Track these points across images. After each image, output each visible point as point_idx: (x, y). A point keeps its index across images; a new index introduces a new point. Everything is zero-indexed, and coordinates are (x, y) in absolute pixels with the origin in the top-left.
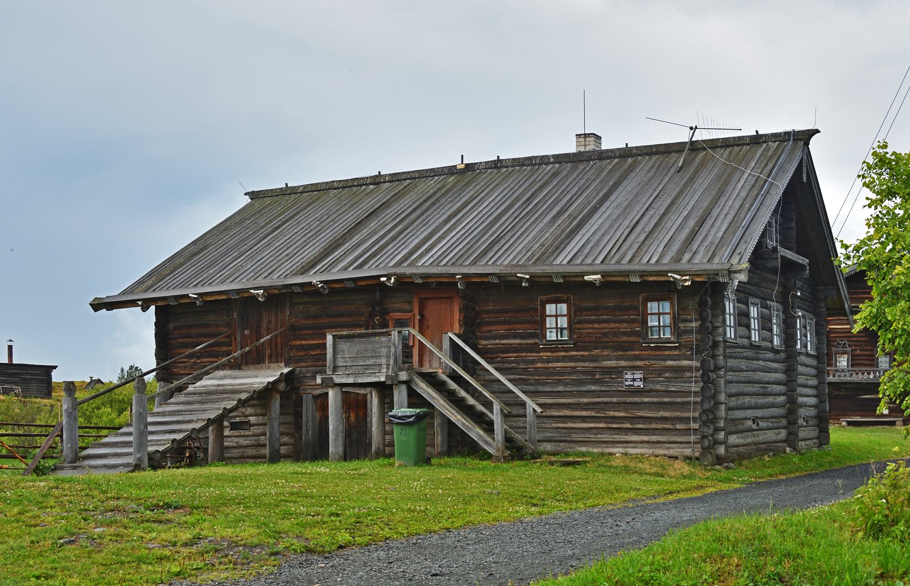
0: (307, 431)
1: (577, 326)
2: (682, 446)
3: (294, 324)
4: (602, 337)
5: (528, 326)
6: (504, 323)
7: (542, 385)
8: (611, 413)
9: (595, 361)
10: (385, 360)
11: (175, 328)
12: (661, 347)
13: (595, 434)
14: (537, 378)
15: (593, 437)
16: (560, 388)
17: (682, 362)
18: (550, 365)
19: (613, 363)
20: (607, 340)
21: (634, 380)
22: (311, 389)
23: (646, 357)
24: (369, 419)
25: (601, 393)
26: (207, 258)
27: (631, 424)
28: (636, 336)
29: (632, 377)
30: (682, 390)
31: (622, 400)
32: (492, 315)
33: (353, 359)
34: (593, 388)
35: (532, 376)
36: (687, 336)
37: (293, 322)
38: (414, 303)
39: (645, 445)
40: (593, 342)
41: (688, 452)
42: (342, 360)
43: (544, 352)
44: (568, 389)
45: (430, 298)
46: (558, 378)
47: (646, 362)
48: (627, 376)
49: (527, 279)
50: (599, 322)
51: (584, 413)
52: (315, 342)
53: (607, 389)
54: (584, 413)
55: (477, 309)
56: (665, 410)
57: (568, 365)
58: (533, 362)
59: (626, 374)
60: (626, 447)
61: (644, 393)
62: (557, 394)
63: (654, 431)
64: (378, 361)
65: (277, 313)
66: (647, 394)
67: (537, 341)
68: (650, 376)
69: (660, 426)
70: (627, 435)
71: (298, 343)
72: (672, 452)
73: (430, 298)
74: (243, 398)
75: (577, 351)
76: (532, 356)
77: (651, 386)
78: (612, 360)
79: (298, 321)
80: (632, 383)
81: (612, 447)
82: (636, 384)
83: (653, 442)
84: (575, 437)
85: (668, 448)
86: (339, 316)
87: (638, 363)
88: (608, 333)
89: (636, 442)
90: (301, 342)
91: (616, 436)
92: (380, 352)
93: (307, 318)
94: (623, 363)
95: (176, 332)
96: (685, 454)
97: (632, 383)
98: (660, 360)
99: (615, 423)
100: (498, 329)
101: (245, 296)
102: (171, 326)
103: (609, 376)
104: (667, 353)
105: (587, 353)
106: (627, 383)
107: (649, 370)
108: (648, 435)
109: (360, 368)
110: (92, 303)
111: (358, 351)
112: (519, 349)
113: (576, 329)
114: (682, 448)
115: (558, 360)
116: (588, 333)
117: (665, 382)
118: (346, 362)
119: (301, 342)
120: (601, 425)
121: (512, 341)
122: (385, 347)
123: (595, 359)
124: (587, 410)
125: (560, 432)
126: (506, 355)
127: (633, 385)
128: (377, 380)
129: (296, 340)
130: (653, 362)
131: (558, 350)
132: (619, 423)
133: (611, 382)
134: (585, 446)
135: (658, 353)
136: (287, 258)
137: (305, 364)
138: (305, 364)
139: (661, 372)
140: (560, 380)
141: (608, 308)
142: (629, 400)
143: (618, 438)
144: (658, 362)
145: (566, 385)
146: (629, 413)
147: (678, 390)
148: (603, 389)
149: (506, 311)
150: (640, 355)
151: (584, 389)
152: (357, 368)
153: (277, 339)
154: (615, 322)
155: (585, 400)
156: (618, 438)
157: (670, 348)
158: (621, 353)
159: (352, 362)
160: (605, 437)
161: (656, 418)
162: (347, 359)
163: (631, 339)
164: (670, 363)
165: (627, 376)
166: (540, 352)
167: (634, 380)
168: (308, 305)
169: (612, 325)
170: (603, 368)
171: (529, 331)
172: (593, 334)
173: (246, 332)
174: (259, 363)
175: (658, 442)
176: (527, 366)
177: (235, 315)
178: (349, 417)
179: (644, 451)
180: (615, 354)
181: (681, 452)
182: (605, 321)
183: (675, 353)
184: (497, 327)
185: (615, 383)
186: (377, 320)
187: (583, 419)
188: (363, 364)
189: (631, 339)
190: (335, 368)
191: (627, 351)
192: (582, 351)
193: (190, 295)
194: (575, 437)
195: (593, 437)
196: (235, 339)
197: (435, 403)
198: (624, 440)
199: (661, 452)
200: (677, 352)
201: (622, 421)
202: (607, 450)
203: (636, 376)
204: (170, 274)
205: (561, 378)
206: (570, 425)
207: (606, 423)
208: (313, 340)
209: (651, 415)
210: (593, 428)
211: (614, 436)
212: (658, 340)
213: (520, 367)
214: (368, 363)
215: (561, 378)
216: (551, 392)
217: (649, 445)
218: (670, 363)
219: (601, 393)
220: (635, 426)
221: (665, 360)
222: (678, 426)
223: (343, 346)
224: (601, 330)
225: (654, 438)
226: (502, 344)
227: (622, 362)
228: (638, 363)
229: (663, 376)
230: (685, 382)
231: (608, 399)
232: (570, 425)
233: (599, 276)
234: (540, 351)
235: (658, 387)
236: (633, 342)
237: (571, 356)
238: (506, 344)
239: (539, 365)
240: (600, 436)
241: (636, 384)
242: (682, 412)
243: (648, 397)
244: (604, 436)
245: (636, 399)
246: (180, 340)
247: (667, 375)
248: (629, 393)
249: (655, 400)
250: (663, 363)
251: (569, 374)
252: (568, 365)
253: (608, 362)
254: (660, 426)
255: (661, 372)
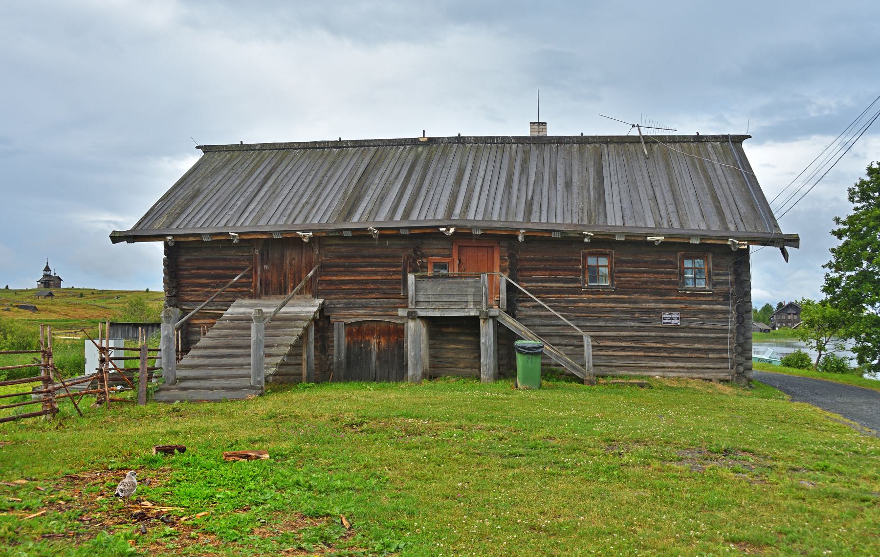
0: (339, 353)
1: (618, 275)
2: (714, 371)
3: (324, 262)
4: (642, 284)
5: (569, 273)
6: (546, 269)
7: (583, 321)
8: (650, 345)
9: (635, 303)
10: (472, 298)
11: (188, 261)
12: (696, 294)
13: (634, 361)
14: (578, 315)
15: (632, 363)
16: (601, 324)
17: (716, 306)
18: (591, 305)
19: (652, 305)
20: (646, 286)
21: (671, 319)
22: (343, 318)
23: (682, 301)
24: (405, 345)
25: (639, 329)
26: (324, 208)
27: (668, 353)
28: (674, 285)
29: (669, 316)
30: (715, 328)
31: (659, 334)
32: (533, 263)
33: (436, 296)
34: (632, 324)
35: (575, 313)
36: (721, 287)
37: (322, 260)
38: (454, 250)
39: (681, 370)
40: (632, 288)
41: (722, 375)
42: (423, 296)
43: (586, 294)
44: (608, 325)
45: (466, 246)
46: (599, 315)
47: (683, 306)
48: (664, 316)
49: (591, 236)
50: (637, 272)
51: (623, 344)
52: (347, 278)
53: (645, 325)
54: (623, 344)
55: (518, 257)
56: (699, 343)
57: (609, 305)
58: (574, 302)
59: (664, 314)
60: (664, 371)
61: (679, 330)
62: (597, 328)
63: (689, 359)
64: (464, 299)
65: (302, 253)
66: (682, 330)
67: (579, 285)
68: (686, 316)
69: (694, 355)
70: (664, 362)
71: (328, 278)
72: (706, 376)
73: (466, 246)
74: (305, 326)
75: (617, 294)
76: (571, 297)
77: (686, 324)
78: (651, 303)
79: (328, 260)
80: (670, 321)
81: (651, 371)
82: (673, 322)
83: (688, 368)
84: (615, 362)
85: (703, 373)
86: (375, 257)
87: (675, 306)
88: (647, 281)
89: (671, 368)
90: (331, 278)
91: (654, 363)
92: (467, 291)
93: (339, 257)
94: (661, 305)
95: (188, 264)
96: (718, 378)
97: (670, 321)
98: (696, 304)
99: (653, 352)
100: (540, 274)
101: (288, 236)
102: (183, 258)
103: (647, 315)
104: (701, 299)
105: (627, 297)
106: (665, 321)
107: (685, 312)
108: (684, 362)
109: (444, 303)
110: (113, 235)
111: (442, 289)
112: (560, 291)
113: (616, 277)
114: (716, 373)
115: (598, 301)
116: (628, 281)
117: (700, 321)
118: (428, 298)
119: (331, 278)
120: (639, 354)
121: (554, 285)
122: (471, 287)
123: (634, 302)
124: (627, 341)
125: (600, 359)
126: (548, 295)
127: (671, 323)
128: (467, 314)
129: (326, 275)
130: (690, 305)
131: (599, 293)
132: (657, 352)
133: (650, 320)
134: (625, 370)
135: (693, 298)
136: (309, 207)
137: (336, 297)
138: (336, 297)
139: (696, 313)
140: (600, 317)
141: (647, 262)
142: (666, 334)
143: (656, 364)
144: (693, 306)
145: (606, 321)
146: (667, 344)
147: (711, 327)
148: (642, 325)
149: (547, 260)
150: (676, 299)
151: (624, 324)
152: (441, 303)
153: (301, 273)
154: (654, 273)
155: (625, 334)
156: (656, 364)
157: (705, 295)
158: (660, 298)
159: (435, 298)
160: (644, 363)
161: (690, 349)
162: (430, 296)
163: (668, 287)
164: (704, 306)
165: (664, 316)
166: (582, 294)
167: (671, 319)
168: (339, 247)
169: (651, 275)
170: (642, 308)
171: (570, 277)
172: (633, 281)
173: (265, 266)
174: (281, 294)
175: (692, 368)
176: (568, 305)
177: (257, 252)
178: (380, 342)
179: (681, 374)
180: (653, 298)
181: (715, 376)
182: (644, 272)
183: (708, 299)
184: (538, 273)
185: (654, 320)
186: (419, 262)
187: (622, 348)
188: (448, 300)
189: (668, 287)
190: (417, 303)
191: (665, 296)
192: (622, 295)
193: (230, 233)
194: (615, 362)
195: (632, 363)
196: (256, 273)
197: (522, 335)
198: (661, 365)
199: (696, 375)
200: (710, 299)
201: (659, 351)
202: (646, 374)
203: (673, 316)
204: (182, 212)
205: (601, 315)
206: (610, 353)
207: (644, 352)
208: (346, 276)
209: (686, 347)
210: (631, 356)
211: (652, 363)
212: (694, 289)
213: (562, 305)
214: (452, 299)
215: (601, 315)
216: (591, 326)
217: (685, 370)
218: (704, 306)
219: (639, 329)
220: (672, 355)
221: (700, 304)
222: (711, 356)
223: (426, 284)
224: (639, 279)
225: (689, 365)
226: (543, 287)
227: (661, 304)
228: (675, 306)
229: (698, 316)
230: (718, 322)
231: (647, 334)
232: (610, 353)
233: (663, 238)
234: (582, 293)
235: (693, 325)
236: (669, 289)
237: (611, 298)
238: (547, 287)
239: (581, 304)
240: (639, 362)
241: (673, 322)
242: (715, 344)
243: (684, 332)
244: (642, 362)
245: (673, 334)
246: (193, 271)
247: (701, 316)
248: (666, 329)
249: (690, 335)
250: (698, 306)
251: (609, 312)
252: (609, 305)
253: (647, 304)
254: (694, 355)
255: (696, 313)
